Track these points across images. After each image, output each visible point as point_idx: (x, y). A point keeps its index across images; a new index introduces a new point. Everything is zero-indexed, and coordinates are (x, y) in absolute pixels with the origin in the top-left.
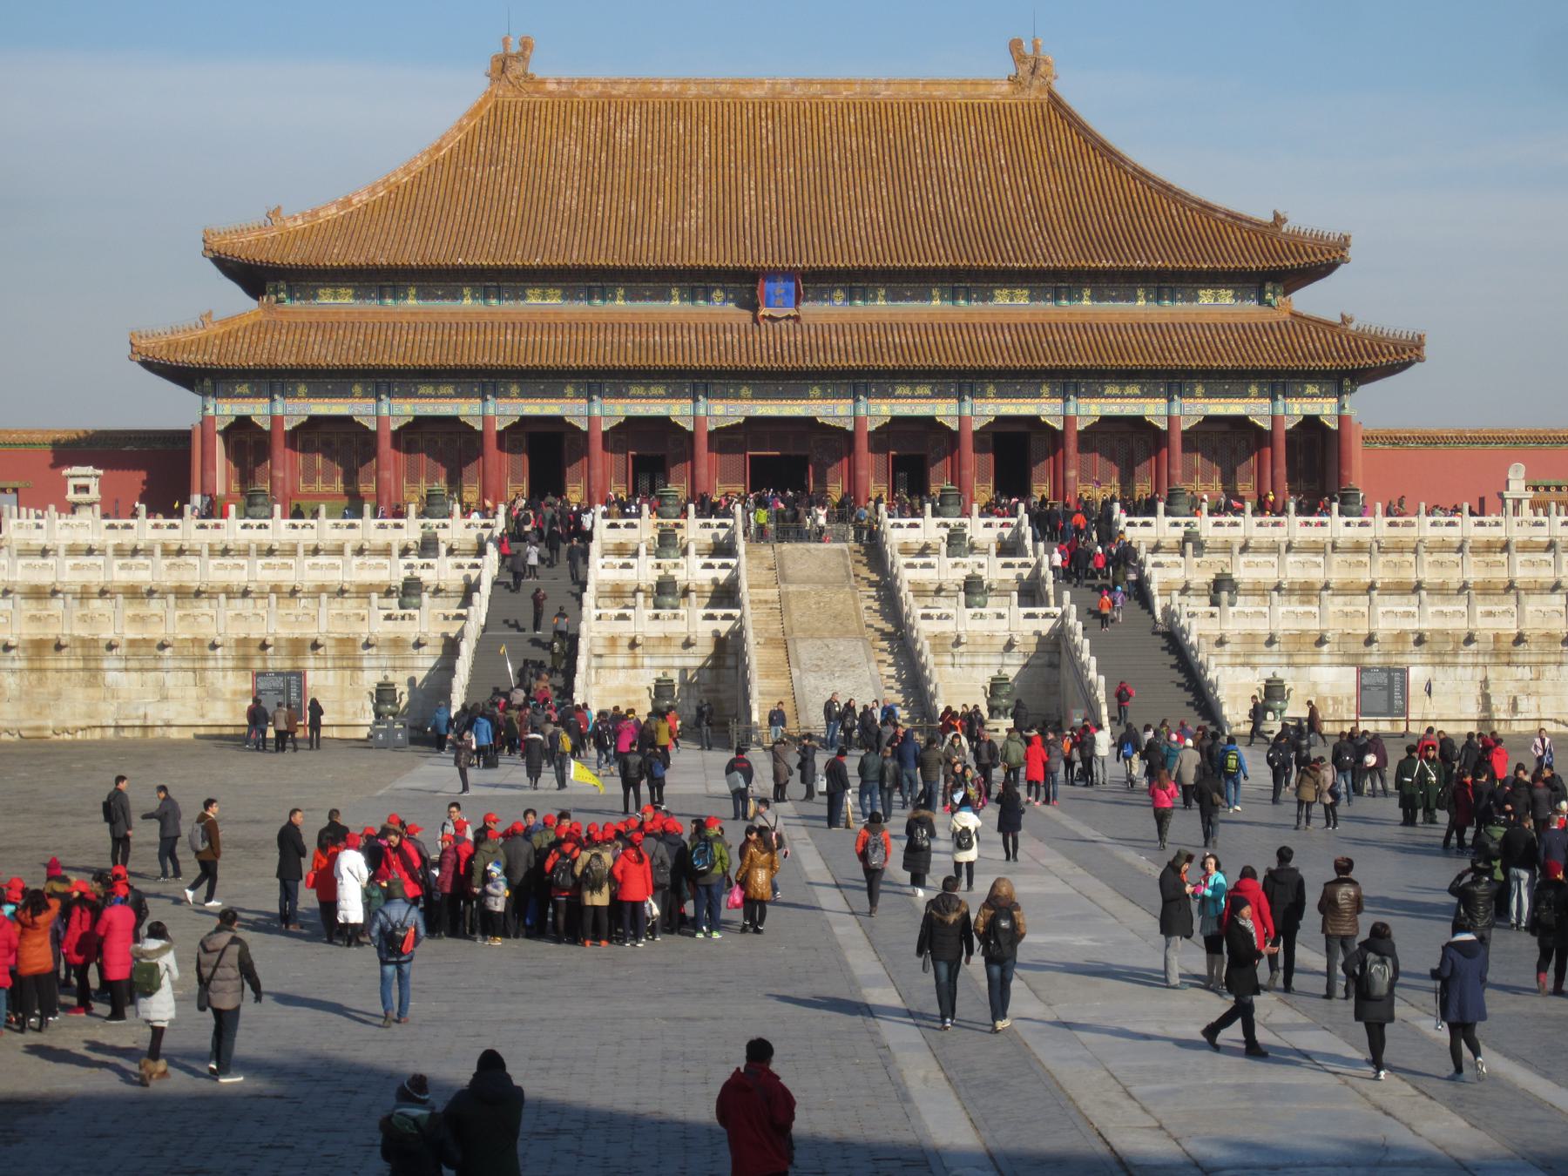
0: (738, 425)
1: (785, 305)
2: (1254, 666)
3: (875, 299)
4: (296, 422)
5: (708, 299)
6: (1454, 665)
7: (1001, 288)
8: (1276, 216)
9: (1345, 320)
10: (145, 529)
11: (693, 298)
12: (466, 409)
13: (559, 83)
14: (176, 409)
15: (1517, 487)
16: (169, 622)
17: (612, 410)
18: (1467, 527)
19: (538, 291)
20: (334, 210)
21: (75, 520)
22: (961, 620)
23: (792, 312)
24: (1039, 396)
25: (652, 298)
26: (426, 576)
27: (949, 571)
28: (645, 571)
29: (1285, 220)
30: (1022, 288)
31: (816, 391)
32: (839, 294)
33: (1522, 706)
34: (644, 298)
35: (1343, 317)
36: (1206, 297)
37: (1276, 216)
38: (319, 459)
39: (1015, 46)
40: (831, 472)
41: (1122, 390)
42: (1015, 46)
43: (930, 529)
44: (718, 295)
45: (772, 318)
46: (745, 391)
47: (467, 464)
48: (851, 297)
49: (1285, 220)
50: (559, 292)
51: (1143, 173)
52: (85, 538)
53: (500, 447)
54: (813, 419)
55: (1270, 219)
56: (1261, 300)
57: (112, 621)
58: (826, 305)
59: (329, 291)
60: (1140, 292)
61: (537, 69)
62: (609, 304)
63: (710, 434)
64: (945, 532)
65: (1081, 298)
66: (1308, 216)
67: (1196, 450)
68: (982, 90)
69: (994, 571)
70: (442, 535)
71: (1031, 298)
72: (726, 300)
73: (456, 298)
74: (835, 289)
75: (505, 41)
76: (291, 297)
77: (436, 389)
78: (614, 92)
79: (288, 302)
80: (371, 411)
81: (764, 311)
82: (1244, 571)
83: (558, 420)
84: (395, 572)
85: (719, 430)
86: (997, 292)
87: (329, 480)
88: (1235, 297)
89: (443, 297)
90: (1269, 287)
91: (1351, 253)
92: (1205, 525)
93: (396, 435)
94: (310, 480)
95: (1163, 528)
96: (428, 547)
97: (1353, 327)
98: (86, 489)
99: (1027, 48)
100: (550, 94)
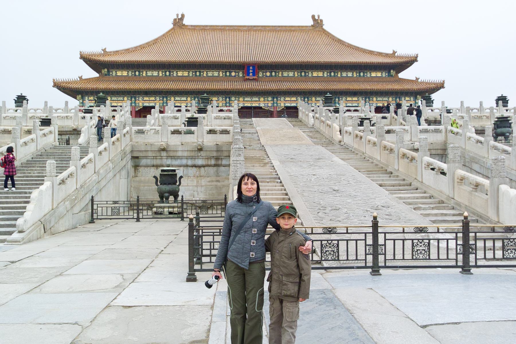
8: (394, 51)
23: (255, 77)
32: (268, 74)
35: (416, 78)
37: (394, 51)
39: (313, 17)
42: (313, 17)
55: (391, 52)
61: (186, 22)
66: (404, 51)
68: (304, 28)
75: (178, 15)
90: (392, 71)
91: (418, 59)
97: (419, 80)
99: (317, 18)
100: (189, 29)
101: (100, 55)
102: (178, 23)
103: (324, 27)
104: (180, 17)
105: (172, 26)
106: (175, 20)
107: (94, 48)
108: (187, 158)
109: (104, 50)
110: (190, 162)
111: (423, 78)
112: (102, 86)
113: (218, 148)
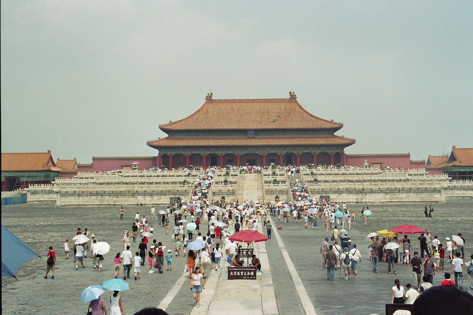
2: (319, 193)
6: (352, 193)
9: (343, 136)
10: (145, 173)
14: (155, 153)
15: (366, 164)
16: (146, 188)
18: (358, 170)
21: (134, 171)
22: (272, 187)
26: (188, 180)
27: (271, 179)
28: (222, 179)
33: (363, 199)
39: (290, 93)
43: (270, 171)
52: (135, 174)
54: (256, 154)
55: (331, 121)
57: (137, 188)
61: (212, 98)
64: (272, 172)
66: (338, 120)
69: (279, 178)
70: (191, 173)
75: (208, 94)
82: (319, 178)
84: (182, 179)
92: (314, 171)
95: (308, 171)
96: (189, 175)
98: (136, 166)
99: (292, 94)
101: (167, 125)
102: (209, 99)
103: (297, 99)
104: (210, 95)
105: (205, 101)
106: (207, 97)
107: (165, 122)
108: (226, 192)
109: (171, 122)
110: (226, 193)
111: (345, 136)
112: (172, 143)
113: (233, 190)
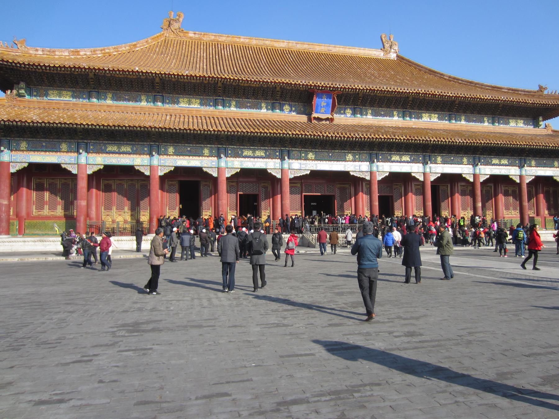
0: (307, 175)
1: (326, 113)
3: (366, 115)
4: (19, 167)
5: (282, 110)
7: (425, 113)
8: (541, 87)
11: (273, 109)
12: (139, 161)
13: (194, 34)
17: (233, 164)
19: (186, 100)
20: (67, 54)
23: (330, 116)
24: (462, 163)
25: (251, 107)
29: (545, 89)
30: (435, 114)
31: (350, 157)
34: (246, 107)
36: (512, 123)
37: (541, 87)
38: (47, 195)
40: (346, 204)
41: (500, 161)
44: (287, 108)
45: (319, 119)
46: (311, 155)
47: (142, 200)
48: (354, 114)
49: (545, 89)
50: (198, 101)
51: (454, 78)
53: (162, 188)
55: (536, 89)
56: (536, 125)
58: (342, 116)
59: (56, 92)
60: (485, 119)
62: (227, 109)
63: (290, 179)
65: (460, 121)
67: (510, 195)
71: (439, 119)
72: (291, 111)
73: (136, 101)
74: (345, 109)
76: (30, 95)
77: (119, 148)
78: (220, 40)
79: (27, 97)
80: (73, 161)
81: (315, 115)
83: (198, 171)
85: (295, 178)
86: (424, 115)
87: (53, 208)
88: (524, 123)
89: (129, 100)
90: (541, 119)
93: (90, 177)
94: (40, 207)
100: (191, 38)
